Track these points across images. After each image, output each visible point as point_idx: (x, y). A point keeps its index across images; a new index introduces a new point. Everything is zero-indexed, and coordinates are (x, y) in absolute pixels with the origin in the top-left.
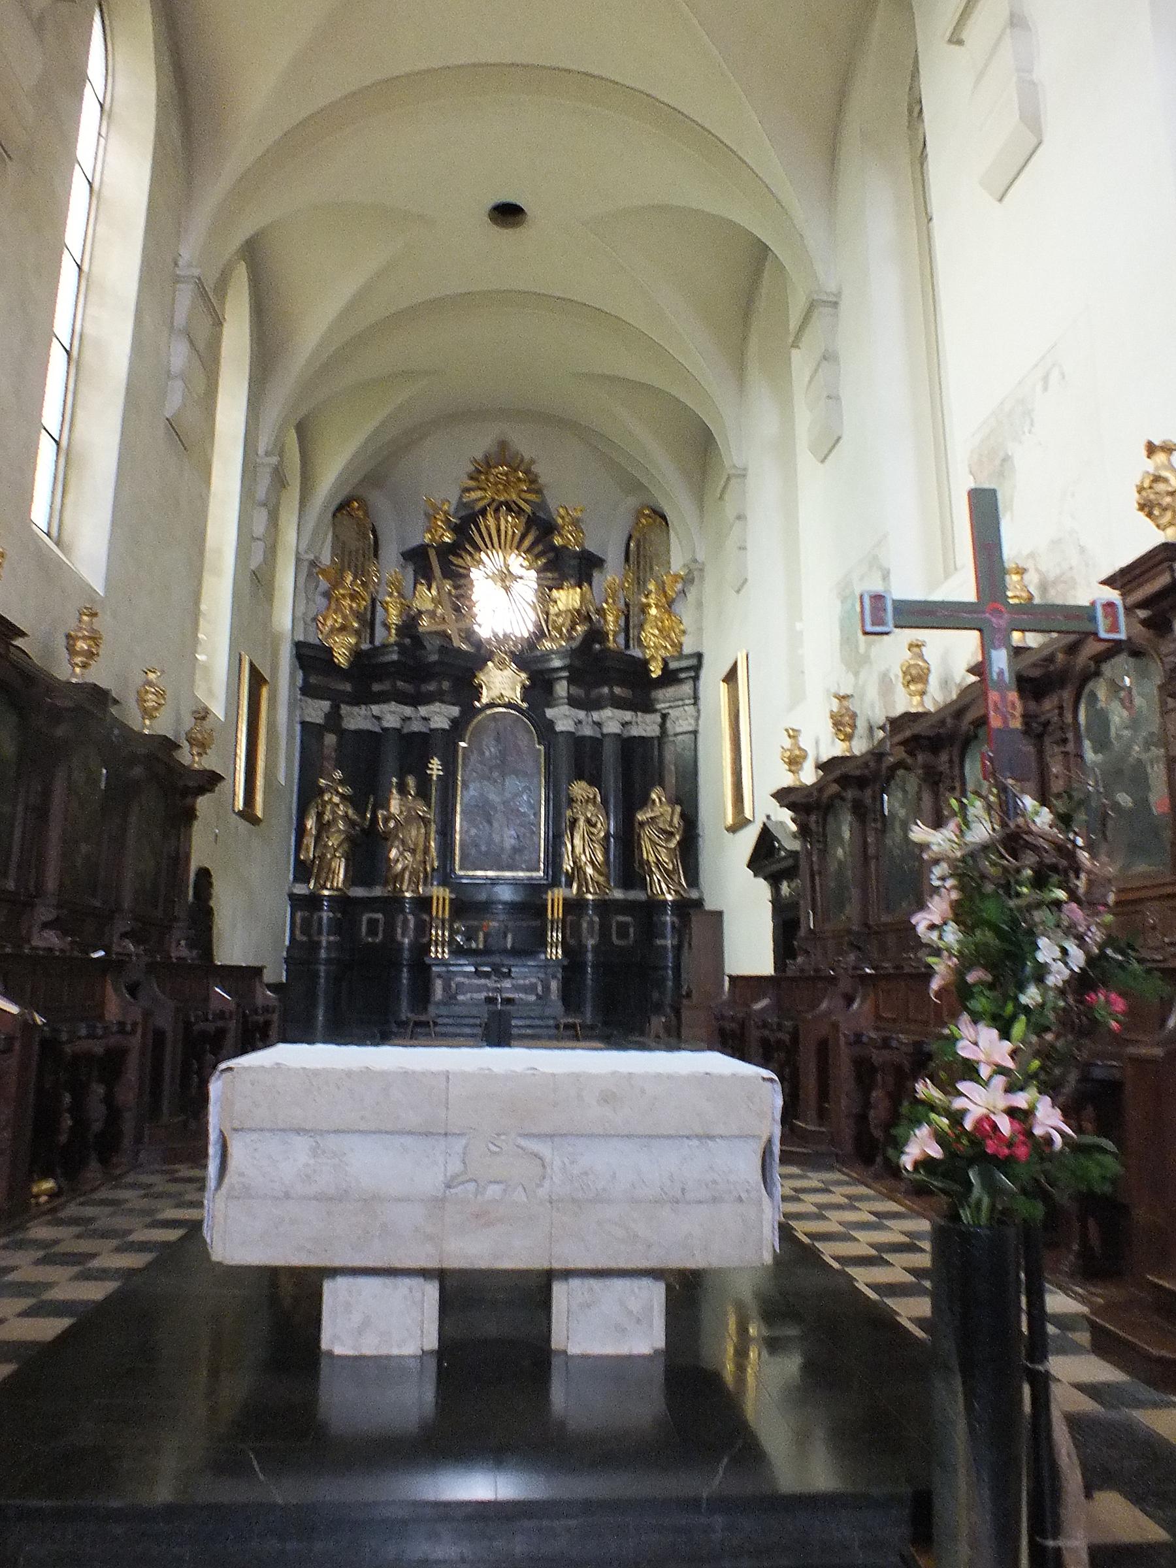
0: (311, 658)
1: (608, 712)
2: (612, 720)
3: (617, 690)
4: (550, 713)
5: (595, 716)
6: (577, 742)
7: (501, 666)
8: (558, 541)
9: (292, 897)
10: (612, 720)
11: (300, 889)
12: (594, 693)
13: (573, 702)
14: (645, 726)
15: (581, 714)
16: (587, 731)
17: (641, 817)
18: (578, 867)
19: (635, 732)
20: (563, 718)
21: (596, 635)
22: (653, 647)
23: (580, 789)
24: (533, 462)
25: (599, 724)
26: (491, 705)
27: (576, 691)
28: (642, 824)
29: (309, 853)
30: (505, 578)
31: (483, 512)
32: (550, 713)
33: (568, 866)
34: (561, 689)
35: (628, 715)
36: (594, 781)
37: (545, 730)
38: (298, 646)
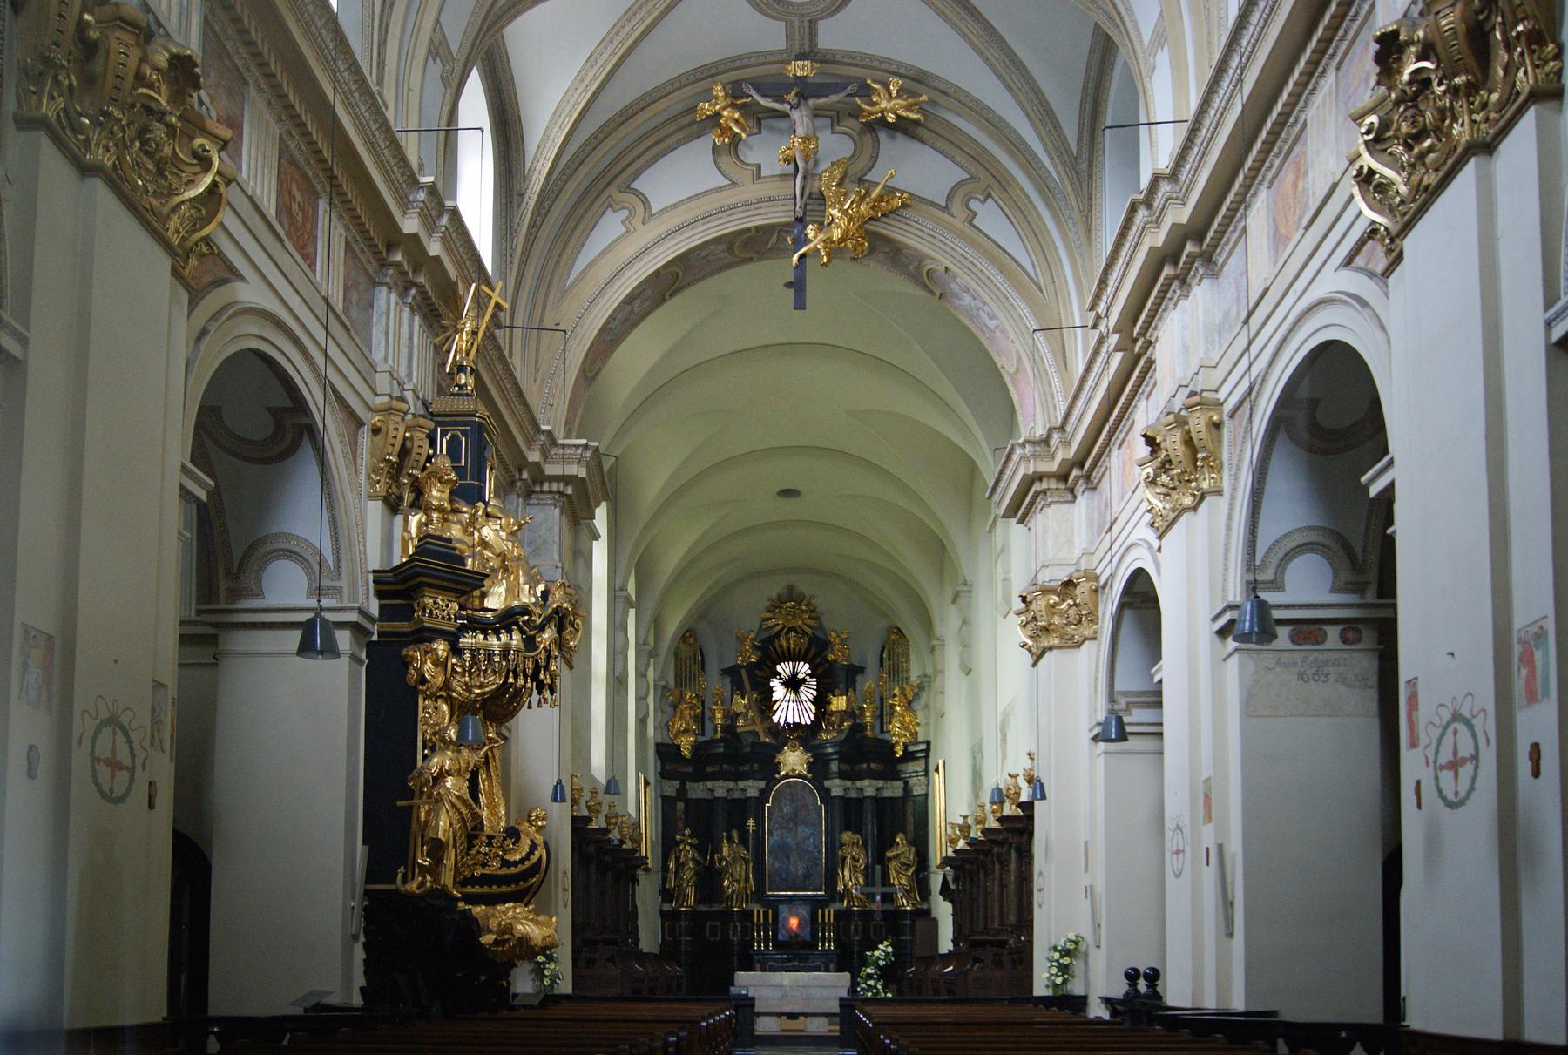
0: (667, 753)
1: (866, 782)
2: (869, 787)
3: (873, 766)
4: (827, 783)
5: (859, 784)
6: (846, 801)
7: (793, 749)
8: (831, 657)
9: (662, 912)
10: (869, 787)
11: (667, 907)
12: (857, 768)
13: (842, 775)
14: (894, 790)
15: (849, 783)
16: (853, 795)
17: (889, 854)
18: (846, 889)
19: (887, 794)
20: (836, 787)
21: (858, 728)
22: (897, 733)
23: (847, 837)
24: (812, 597)
25: (861, 790)
26: (787, 776)
27: (843, 767)
28: (890, 859)
29: (671, 884)
30: (793, 684)
31: (777, 635)
32: (827, 783)
33: (840, 888)
34: (834, 766)
35: (881, 783)
36: (858, 831)
37: (825, 794)
38: (658, 745)
